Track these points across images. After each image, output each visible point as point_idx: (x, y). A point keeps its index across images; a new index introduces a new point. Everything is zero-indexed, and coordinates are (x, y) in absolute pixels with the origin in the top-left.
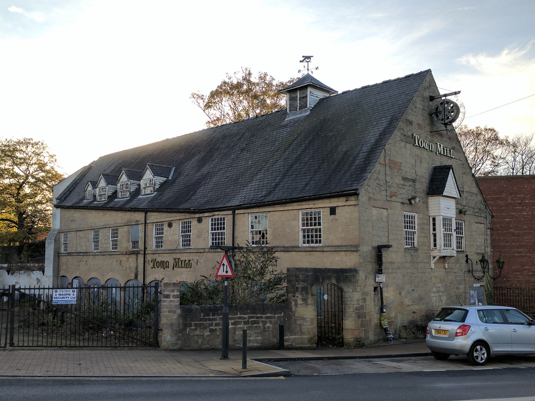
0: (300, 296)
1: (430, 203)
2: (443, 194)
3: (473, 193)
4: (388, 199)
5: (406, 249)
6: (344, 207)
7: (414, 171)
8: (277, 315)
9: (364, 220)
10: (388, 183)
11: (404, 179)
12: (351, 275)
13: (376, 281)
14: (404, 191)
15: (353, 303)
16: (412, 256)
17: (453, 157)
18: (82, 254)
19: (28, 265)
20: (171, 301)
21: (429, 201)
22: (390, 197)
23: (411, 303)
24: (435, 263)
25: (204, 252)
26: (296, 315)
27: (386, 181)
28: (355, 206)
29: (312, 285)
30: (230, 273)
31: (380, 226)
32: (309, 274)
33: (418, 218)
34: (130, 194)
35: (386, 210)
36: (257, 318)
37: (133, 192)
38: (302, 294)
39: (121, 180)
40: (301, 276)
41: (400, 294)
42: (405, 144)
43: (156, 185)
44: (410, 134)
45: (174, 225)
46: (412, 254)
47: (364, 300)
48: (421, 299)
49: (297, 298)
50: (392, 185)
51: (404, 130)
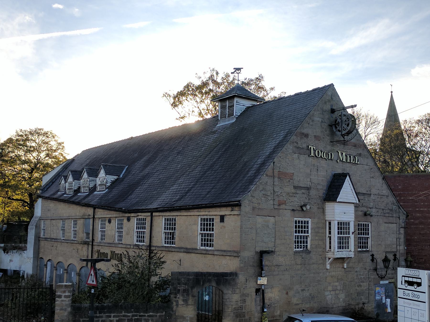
0: (181, 297)
1: (326, 208)
2: (336, 201)
3: (383, 195)
4: (276, 207)
5: (296, 252)
6: (230, 216)
7: (309, 180)
8: (159, 314)
9: (246, 228)
10: (277, 193)
11: (295, 187)
12: (231, 279)
13: (258, 283)
14: (296, 199)
15: (232, 304)
16: (303, 258)
17: (358, 163)
18: (53, 240)
19: (21, 245)
20: (62, 301)
21: (326, 206)
22: (278, 206)
23: (300, 302)
24: (331, 264)
25: (130, 248)
26: (177, 314)
27: (274, 191)
28: (238, 216)
29: (192, 288)
30: (95, 283)
31: (266, 232)
32: (191, 277)
33: (312, 222)
34: (89, 189)
35: (273, 217)
36: (140, 316)
37: (92, 188)
38: (183, 295)
39: (83, 177)
40: (183, 279)
41: (287, 293)
42: (298, 155)
43: (108, 183)
44: (305, 146)
45: (112, 221)
46: (304, 256)
47: (244, 301)
48: (313, 297)
49: (178, 299)
50: (281, 194)
51: (297, 143)
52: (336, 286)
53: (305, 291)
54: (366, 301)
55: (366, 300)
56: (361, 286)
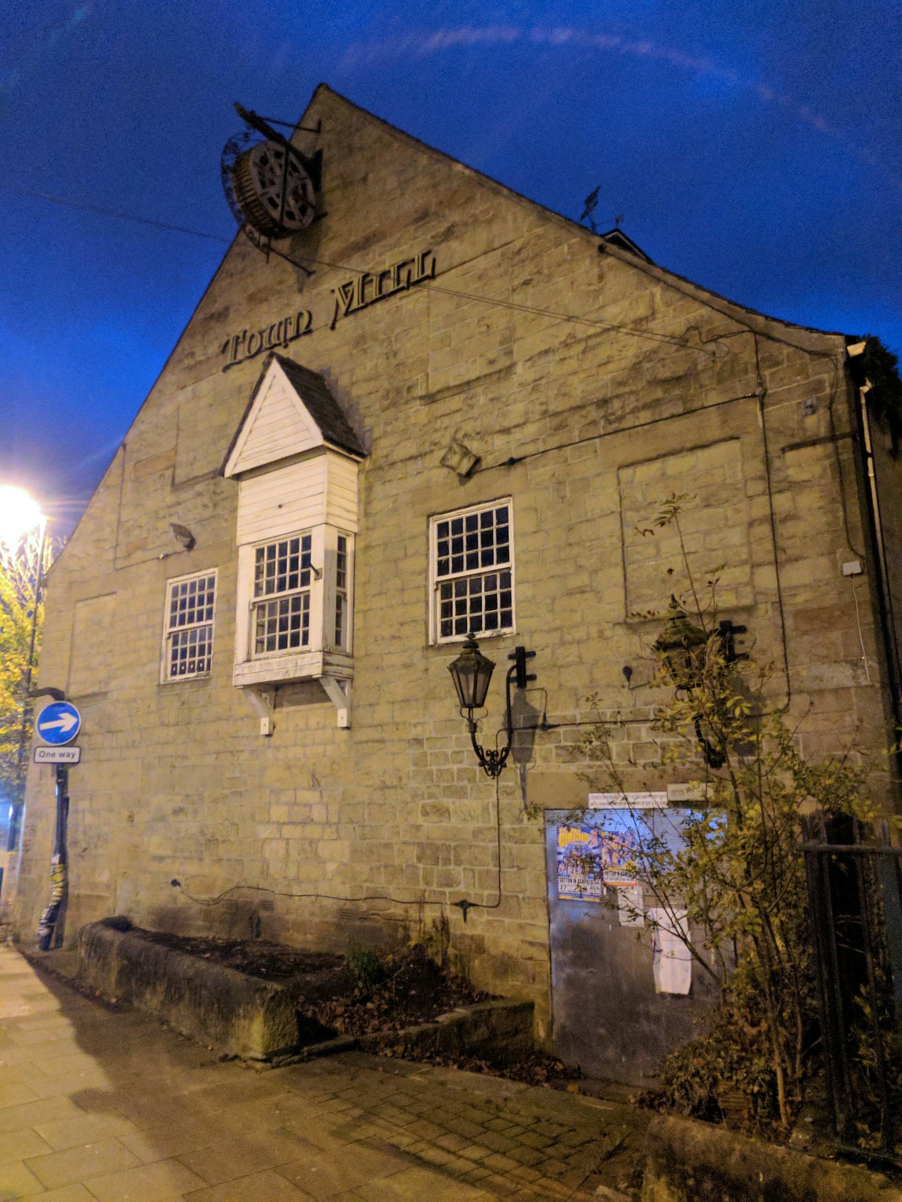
4: (120, 564)
23: (169, 852)
41: (131, 818)
46: (185, 697)
48: (212, 841)
52: (306, 805)
53: (186, 815)
54: (486, 893)
55: (481, 886)
56: (443, 812)
